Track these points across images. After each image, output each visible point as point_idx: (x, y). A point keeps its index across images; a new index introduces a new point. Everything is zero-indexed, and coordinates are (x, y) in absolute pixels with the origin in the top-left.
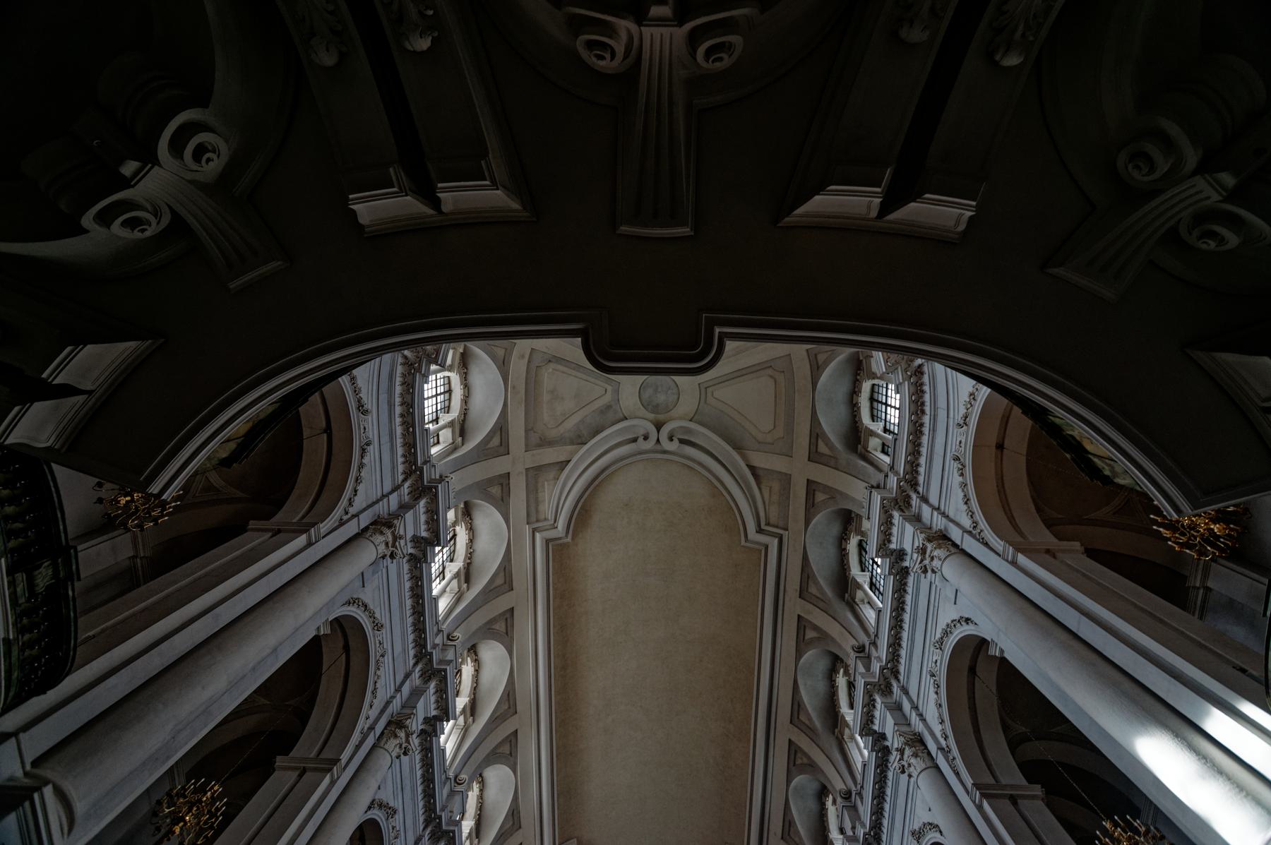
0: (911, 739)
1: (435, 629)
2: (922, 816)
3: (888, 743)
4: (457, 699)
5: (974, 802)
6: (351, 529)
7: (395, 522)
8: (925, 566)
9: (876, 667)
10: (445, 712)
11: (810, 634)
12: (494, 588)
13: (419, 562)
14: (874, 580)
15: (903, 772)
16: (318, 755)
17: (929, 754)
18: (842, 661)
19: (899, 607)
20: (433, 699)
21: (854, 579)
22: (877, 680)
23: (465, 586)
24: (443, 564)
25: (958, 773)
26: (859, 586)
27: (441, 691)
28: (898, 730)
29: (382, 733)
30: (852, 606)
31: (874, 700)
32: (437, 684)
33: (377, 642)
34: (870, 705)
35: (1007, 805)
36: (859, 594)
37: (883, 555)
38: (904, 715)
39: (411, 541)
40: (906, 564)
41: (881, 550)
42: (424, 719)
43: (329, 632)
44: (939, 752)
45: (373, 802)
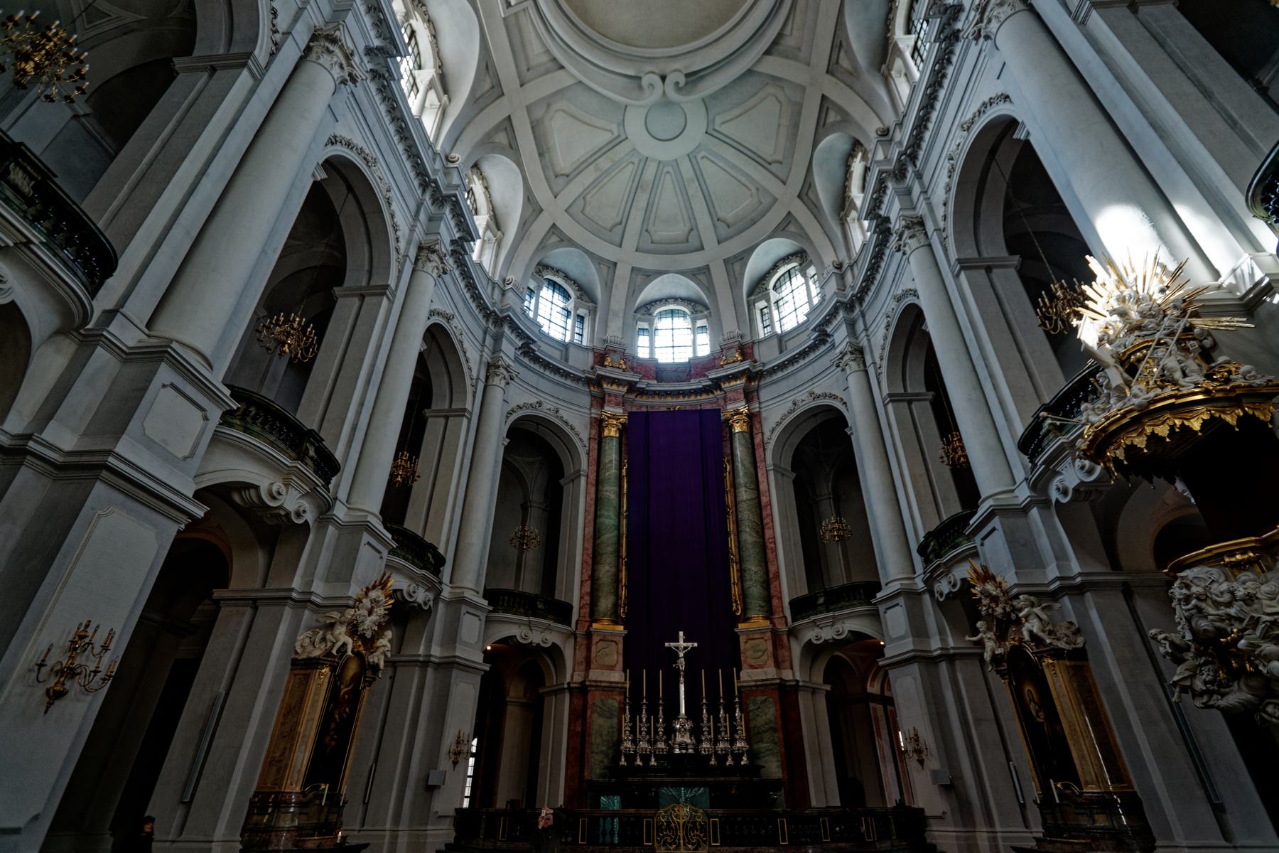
1: (430, 152)
2: (906, 284)
3: (892, 226)
4: (475, 217)
5: (953, 273)
6: (290, 53)
7: (337, 33)
8: (980, 30)
9: (895, 152)
10: (467, 235)
11: (832, 117)
12: (482, 95)
13: (385, 79)
14: (919, 43)
15: (899, 250)
17: (926, 234)
18: (861, 145)
19: (936, 81)
20: (452, 223)
21: (896, 45)
22: (892, 167)
23: (445, 98)
24: (411, 73)
26: (900, 53)
28: (902, 215)
29: (417, 260)
30: (887, 80)
31: (886, 187)
32: (452, 209)
33: (377, 178)
34: (881, 189)
35: (981, 275)
36: (898, 63)
37: (934, 14)
38: (911, 201)
39: (366, 55)
40: (959, 25)
41: (934, 7)
42: (451, 241)
43: (324, 176)
44: (935, 233)
45: (431, 311)
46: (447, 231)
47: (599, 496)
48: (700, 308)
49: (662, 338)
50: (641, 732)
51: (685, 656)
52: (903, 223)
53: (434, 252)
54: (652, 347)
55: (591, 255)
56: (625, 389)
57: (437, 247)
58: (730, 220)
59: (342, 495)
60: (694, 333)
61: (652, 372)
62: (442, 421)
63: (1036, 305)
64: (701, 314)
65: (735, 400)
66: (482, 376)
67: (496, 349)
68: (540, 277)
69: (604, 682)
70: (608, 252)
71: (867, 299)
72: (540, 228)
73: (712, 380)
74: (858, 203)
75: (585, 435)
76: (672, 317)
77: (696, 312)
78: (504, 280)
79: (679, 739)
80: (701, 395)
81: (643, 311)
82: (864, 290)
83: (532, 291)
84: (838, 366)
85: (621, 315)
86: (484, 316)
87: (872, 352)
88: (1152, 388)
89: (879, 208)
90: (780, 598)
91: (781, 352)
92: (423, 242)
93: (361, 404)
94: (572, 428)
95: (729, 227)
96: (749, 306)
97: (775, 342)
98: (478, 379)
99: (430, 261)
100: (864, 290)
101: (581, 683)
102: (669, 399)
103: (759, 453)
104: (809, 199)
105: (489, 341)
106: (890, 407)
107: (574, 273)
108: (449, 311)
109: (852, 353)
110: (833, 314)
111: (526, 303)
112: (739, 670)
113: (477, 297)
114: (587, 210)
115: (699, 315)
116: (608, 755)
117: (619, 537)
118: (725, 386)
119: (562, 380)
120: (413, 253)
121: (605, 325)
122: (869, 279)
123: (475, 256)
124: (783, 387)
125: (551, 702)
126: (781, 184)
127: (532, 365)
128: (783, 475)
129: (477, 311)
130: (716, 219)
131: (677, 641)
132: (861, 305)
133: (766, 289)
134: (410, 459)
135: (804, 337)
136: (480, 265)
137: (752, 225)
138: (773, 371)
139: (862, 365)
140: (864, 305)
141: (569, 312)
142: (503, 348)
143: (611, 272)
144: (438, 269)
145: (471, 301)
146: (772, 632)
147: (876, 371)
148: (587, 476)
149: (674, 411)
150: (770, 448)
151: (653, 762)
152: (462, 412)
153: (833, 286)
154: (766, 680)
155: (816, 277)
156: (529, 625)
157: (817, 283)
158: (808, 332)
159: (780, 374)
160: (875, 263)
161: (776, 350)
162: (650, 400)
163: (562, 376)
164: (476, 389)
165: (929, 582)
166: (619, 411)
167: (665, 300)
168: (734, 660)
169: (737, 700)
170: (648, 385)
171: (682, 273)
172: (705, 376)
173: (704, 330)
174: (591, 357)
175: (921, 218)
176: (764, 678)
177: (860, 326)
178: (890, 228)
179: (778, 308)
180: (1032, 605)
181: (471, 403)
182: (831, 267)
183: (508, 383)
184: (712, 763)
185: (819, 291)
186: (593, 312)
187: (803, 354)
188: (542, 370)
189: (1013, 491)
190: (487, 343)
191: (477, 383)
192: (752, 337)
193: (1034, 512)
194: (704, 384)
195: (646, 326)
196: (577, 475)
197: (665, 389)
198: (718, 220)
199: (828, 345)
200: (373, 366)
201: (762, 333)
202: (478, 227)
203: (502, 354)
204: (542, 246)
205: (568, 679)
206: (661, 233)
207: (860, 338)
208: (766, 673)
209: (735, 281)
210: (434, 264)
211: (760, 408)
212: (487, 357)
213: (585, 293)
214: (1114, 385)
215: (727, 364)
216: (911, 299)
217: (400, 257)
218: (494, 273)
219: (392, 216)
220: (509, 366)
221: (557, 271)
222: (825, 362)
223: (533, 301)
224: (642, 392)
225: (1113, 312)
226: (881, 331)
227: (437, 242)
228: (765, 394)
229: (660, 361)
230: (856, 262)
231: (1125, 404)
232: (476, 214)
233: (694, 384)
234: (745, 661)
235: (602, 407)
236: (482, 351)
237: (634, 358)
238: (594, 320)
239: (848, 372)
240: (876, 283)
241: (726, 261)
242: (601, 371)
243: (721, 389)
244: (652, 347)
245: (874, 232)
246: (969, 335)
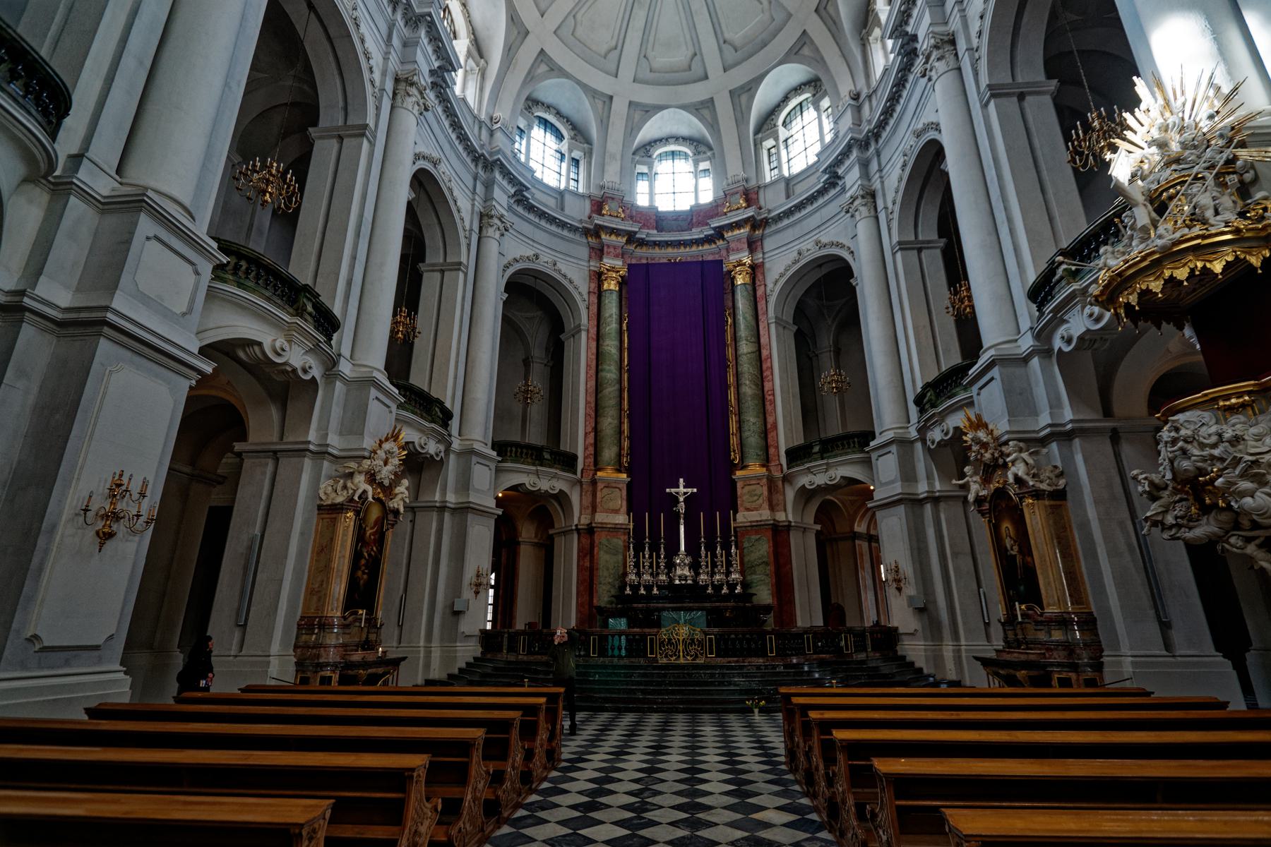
0: (941, 40)
2: (928, 117)
3: (918, 46)
5: (981, 102)
10: (447, 64)
15: (924, 76)
16: (345, 123)
17: (956, 55)
20: (430, 49)
25: (977, 74)
27: (435, 39)
28: (932, 32)
29: (395, 94)
44: (967, 53)
46: (425, 61)
47: (600, 350)
48: (703, 148)
49: (662, 184)
50: (644, 567)
52: (932, 41)
53: (412, 84)
54: (652, 194)
55: (585, 87)
56: (624, 240)
57: (415, 78)
58: (738, 43)
59: (345, 351)
60: (696, 177)
61: (652, 221)
62: (438, 275)
63: (1067, 138)
64: (704, 156)
65: (738, 250)
66: (476, 227)
67: (488, 198)
68: (530, 115)
69: (610, 524)
70: (602, 83)
71: (884, 135)
72: (527, 55)
73: (714, 229)
74: (883, 17)
75: (584, 289)
76: (673, 159)
77: (699, 153)
78: (491, 119)
79: (679, 572)
80: (702, 246)
81: (641, 152)
82: (882, 124)
83: (522, 131)
84: (847, 212)
85: (619, 157)
86: (473, 160)
87: (884, 195)
88: (1179, 228)
89: (907, 23)
90: (777, 447)
91: (788, 197)
92: (399, 72)
93: (354, 258)
94: (571, 282)
95: (736, 51)
96: (755, 145)
97: (782, 185)
98: (471, 230)
99: (409, 95)
100: (882, 124)
101: (588, 525)
102: (670, 250)
103: (761, 305)
104: (828, 13)
105: (480, 188)
106: (899, 255)
107: (566, 109)
108: (435, 155)
109: (863, 197)
110: (845, 154)
111: (517, 145)
112: (736, 512)
113: (463, 138)
114: (579, 33)
115: (702, 156)
116: (614, 586)
117: (621, 391)
118: (728, 235)
119: (559, 231)
120: (389, 86)
121: (602, 169)
122: (888, 112)
123: (458, 90)
124: (788, 235)
125: (560, 543)
127: (527, 215)
128: (784, 328)
129: (464, 155)
130: (721, 42)
132: (877, 141)
133: (775, 126)
134: (409, 315)
135: (813, 179)
136: (464, 100)
137: (762, 48)
138: (779, 218)
139: (872, 210)
140: (881, 141)
141: (563, 155)
142: (495, 196)
143: (606, 108)
144: (419, 105)
145: (457, 143)
146: (768, 479)
147: (887, 217)
148: (588, 330)
149: (675, 262)
150: (772, 300)
151: (655, 591)
152: (458, 266)
153: (848, 120)
154: (761, 521)
155: (830, 110)
156: (537, 473)
157: (831, 117)
158: (819, 174)
159: (786, 222)
160: (896, 92)
161: (783, 195)
162: (651, 251)
163: (558, 226)
164: (470, 241)
165: (922, 431)
166: (618, 263)
168: (732, 504)
169: (733, 538)
170: (648, 235)
171: (684, 107)
172: (707, 224)
173: (707, 174)
174: (587, 206)
175: (953, 35)
176: (759, 519)
177: (874, 166)
178: (916, 49)
179: (787, 147)
180: (1021, 450)
181: (466, 256)
182: (848, 98)
183: (502, 235)
184: (709, 591)
185: (832, 126)
186: (588, 154)
187: (811, 199)
188: (537, 220)
189: (1016, 340)
190: (478, 190)
191: (471, 234)
192: (757, 181)
193: (1035, 362)
194: (705, 233)
195: (644, 169)
196: (578, 330)
197: (666, 239)
198: (725, 42)
199: (838, 189)
200: (361, 216)
201: (768, 176)
202: (458, 54)
203: (494, 203)
204: (530, 77)
205: (576, 522)
206: (662, 59)
207: (873, 180)
209: (741, 116)
210: (414, 99)
211: (764, 259)
212: (479, 206)
213: (579, 133)
214: (1139, 226)
215: (730, 211)
216: (932, 135)
217: (376, 90)
218: (480, 109)
219: (363, 41)
220: (502, 216)
221: (548, 107)
222: (833, 208)
223: (524, 142)
224: (642, 243)
225: (1150, 144)
226: (897, 171)
227: (415, 72)
228: (769, 244)
229: (660, 209)
230: (875, 91)
231: (1147, 246)
232: (455, 38)
233: (696, 234)
234: (742, 505)
235: (601, 259)
236: (473, 200)
237: (633, 205)
238: (589, 163)
239: (858, 218)
240: (895, 115)
242: (598, 221)
243: (724, 239)
244: (652, 194)
245: (898, 55)
246: (991, 174)
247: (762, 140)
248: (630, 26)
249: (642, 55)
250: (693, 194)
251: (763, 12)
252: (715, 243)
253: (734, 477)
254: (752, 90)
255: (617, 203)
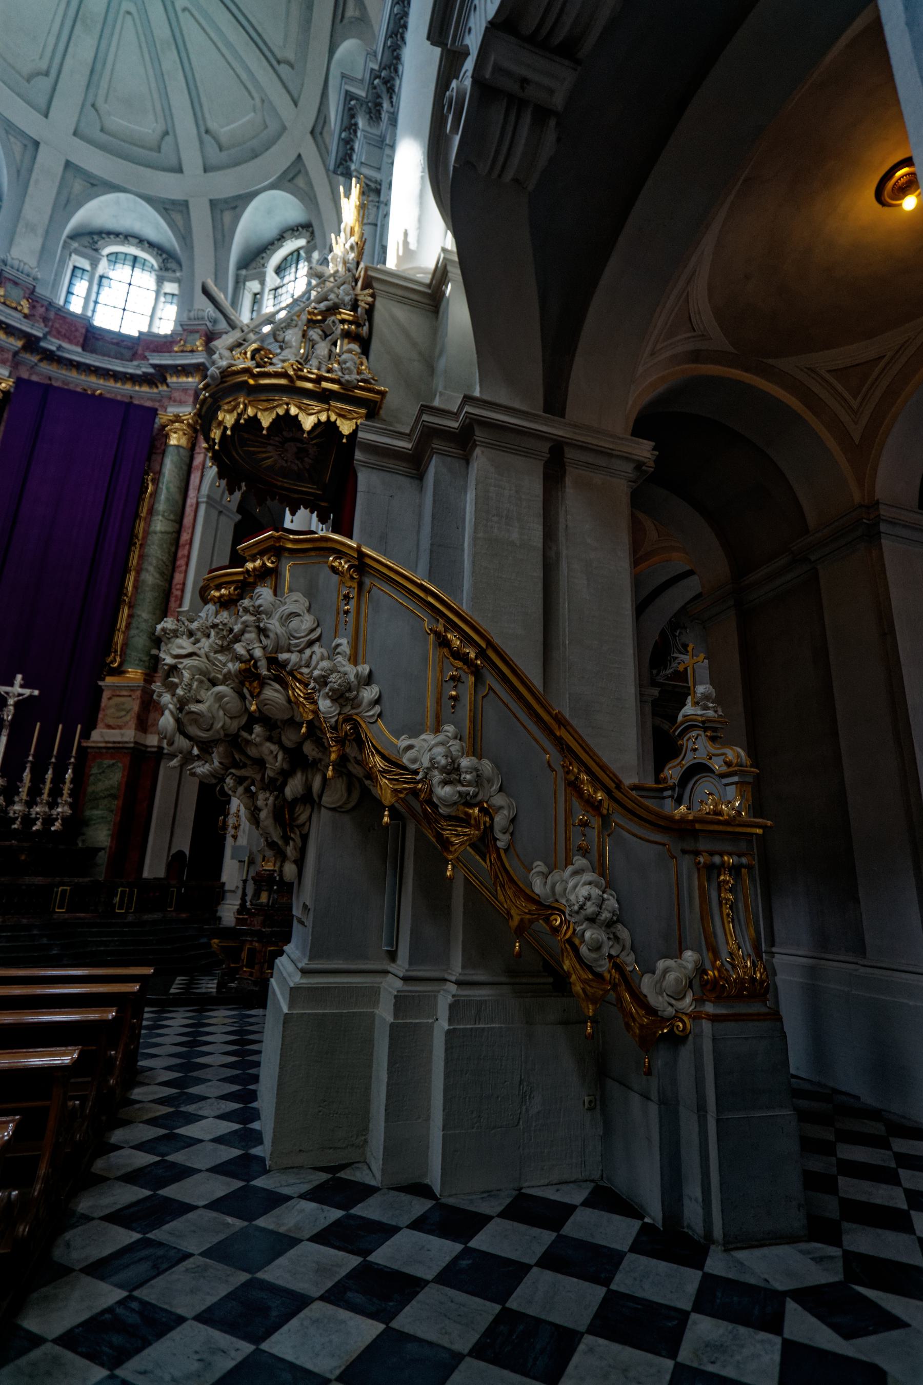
51: (17, 705)
58: (224, 140)
61: (77, 334)
65: (181, 403)
76: (133, 267)
77: (167, 269)
81: (86, 240)
85: (41, 231)
95: (221, 150)
102: (93, 379)
115: (169, 274)
118: (172, 380)
126: (292, 103)
130: (202, 129)
131: (12, 685)
146: (142, 690)
149: (93, 395)
162: (64, 372)
167: (126, 237)
170: (60, 348)
171: (149, 200)
184: (15, 826)
194: (144, 370)
208: (122, 735)
224: (50, 357)
234: (103, 720)
241: (213, 203)
247: (245, 280)
248: (70, 50)
249: (88, 104)
250: (149, 319)
251: (255, 111)
252: (157, 387)
253: (100, 683)
254: (238, 209)
255: (22, 293)
